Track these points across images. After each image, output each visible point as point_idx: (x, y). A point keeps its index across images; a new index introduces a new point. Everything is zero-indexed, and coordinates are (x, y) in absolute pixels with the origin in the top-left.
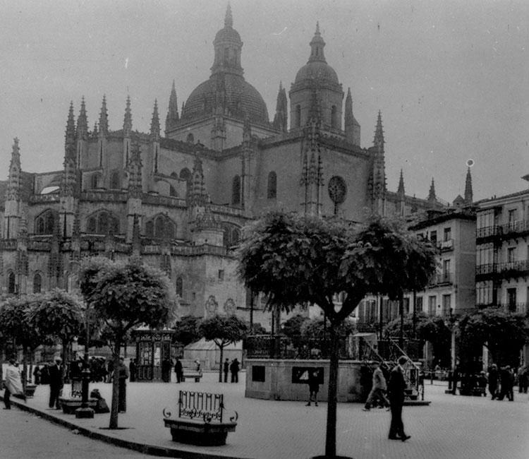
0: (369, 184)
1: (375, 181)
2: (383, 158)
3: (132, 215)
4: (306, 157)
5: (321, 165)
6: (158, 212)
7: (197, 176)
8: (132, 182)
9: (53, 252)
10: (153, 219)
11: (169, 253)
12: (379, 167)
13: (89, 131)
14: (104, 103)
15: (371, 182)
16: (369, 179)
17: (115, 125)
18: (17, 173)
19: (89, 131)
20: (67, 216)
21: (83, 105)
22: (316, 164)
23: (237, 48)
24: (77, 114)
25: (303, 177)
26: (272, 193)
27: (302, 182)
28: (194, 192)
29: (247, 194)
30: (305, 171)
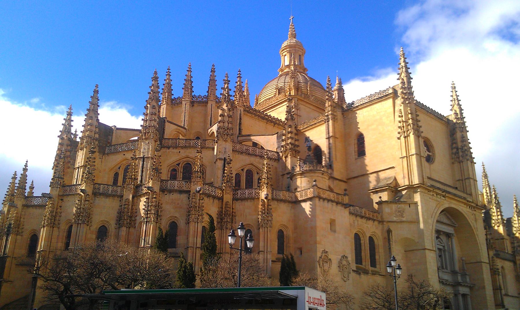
0: (452, 149)
1: (460, 144)
2: (464, 123)
3: (220, 159)
5: (418, 118)
6: (248, 162)
12: (462, 132)
15: (454, 146)
16: (452, 144)
17: (200, 89)
18: (95, 123)
20: (145, 160)
22: (414, 116)
23: (301, 53)
25: (399, 130)
26: (361, 152)
30: (400, 125)
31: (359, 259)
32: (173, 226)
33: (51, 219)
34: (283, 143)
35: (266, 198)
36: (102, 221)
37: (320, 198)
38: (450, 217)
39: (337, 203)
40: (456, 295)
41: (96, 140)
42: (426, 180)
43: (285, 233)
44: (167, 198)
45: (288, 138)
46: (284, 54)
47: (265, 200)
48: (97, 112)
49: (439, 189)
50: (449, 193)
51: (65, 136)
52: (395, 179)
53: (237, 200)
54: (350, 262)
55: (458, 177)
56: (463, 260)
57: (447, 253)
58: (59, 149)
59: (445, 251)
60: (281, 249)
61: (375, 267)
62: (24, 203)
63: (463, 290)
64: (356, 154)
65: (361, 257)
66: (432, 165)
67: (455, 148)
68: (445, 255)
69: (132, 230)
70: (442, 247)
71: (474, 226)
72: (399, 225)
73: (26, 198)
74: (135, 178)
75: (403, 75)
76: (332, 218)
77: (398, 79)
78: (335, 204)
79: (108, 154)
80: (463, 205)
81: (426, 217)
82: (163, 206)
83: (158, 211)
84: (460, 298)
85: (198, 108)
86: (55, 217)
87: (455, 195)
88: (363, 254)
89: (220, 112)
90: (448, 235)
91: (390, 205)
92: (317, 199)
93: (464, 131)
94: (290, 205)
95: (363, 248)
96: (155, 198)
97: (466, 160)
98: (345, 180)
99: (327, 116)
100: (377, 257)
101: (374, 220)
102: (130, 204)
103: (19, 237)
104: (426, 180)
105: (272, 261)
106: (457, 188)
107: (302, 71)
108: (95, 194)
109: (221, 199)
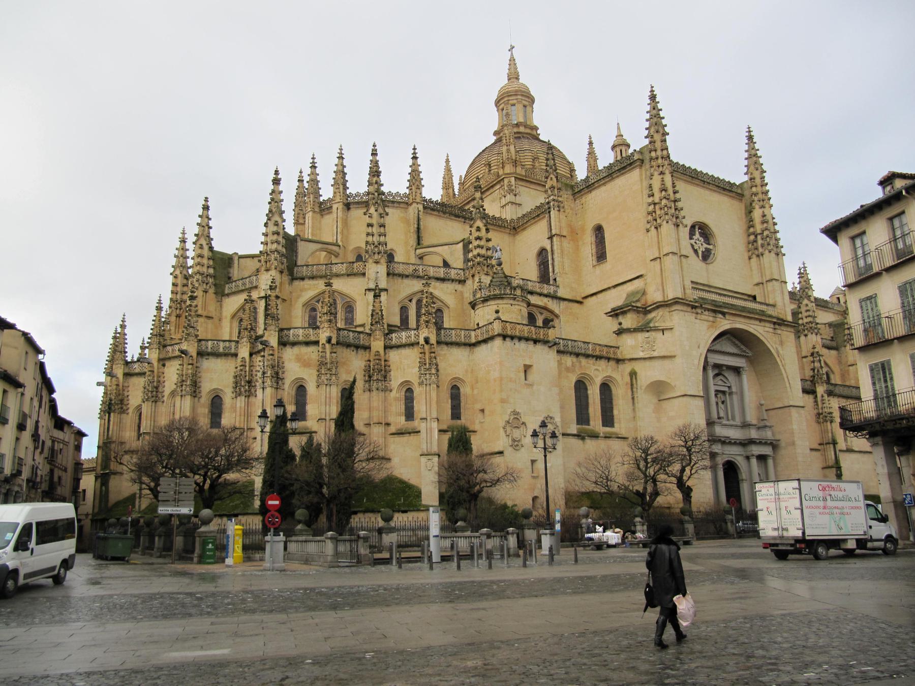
1: (759, 228)
3: (369, 290)
4: (650, 186)
5: (678, 196)
7: (478, 229)
8: (370, 239)
9: (240, 356)
10: (410, 301)
11: (433, 340)
12: (763, 207)
13: (321, 199)
14: (341, 158)
15: (752, 230)
17: (358, 185)
18: (206, 252)
19: (321, 199)
21: (314, 167)
23: (527, 103)
24: (306, 178)
25: (650, 218)
26: (601, 256)
27: (648, 226)
28: (475, 252)
29: (560, 265)
30: (651, 208)
31: (583, 416)
32: (301, 390)
33: (152, 392)
34: (470, 255)
35: (427, 340)
36: (214, 389)
37: (504, 337)
38: (737, 342)
39: (535, 342)
40: (748, 458)
41: (211, 276)
42: (689, 291)
43: (461, 390)
44: (289, 354)
45: (476, 248)
46: (501, 107)
47: (427, 347)
48: (209, 237)
49: (713, 303)
50: (733, 306)
51: (178, 272)
52: (644, 293)
53: (392, 347)
54: (559, 424)
55: (757, 280)
56: (762, 405)
57: (735, 397)
58: (172, 292)
59: (731, 394)
60: (456, 413)
61: (612, 425)
62: (127, 371)
63: (757, 450)
64: (594, 258)
65: (588, 414)
66: (710, 266)
67: (753, 233)
68: (731, 399)
69: (252, 399)
70: (726, 389)
71: (778, 352)
72: (648, 363)
73: (127, 363)
74: (252, 329)
75: (652, 130)
76: (528, 363)
77: (646, 137)
78: (532, 342)
79: (228, 295)
80: (757, 322)
81: (687, 348)
82: (286, 364)
83: (277, 373)
84: (754, 461)
85: (357, 213)
86: (157, 388)
87: (744, 309)
88: (591, 410)
89: (368, 220)
90: (737, 370)
91: (635, 334)
92: (501, 338)
93: (767, 206)
94: (468, 349)
95: (591, 401)
96: (272, 355)
97: (767, 252)
98: (579, 299)
99: (548, 203)
100: (615, 412)
101: (609, 359)
102: (247, 364)
103: (124, 416)
104: (689, 291)
105: (440, 431)
106: (754, 297)
107: (528, 131)
108: (201, 354)
109: (367, 348)
